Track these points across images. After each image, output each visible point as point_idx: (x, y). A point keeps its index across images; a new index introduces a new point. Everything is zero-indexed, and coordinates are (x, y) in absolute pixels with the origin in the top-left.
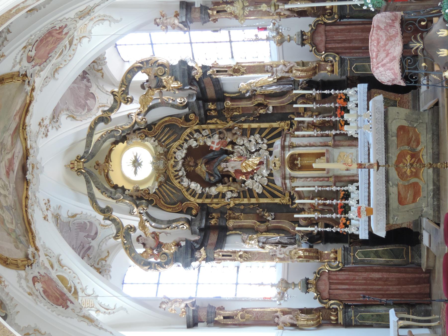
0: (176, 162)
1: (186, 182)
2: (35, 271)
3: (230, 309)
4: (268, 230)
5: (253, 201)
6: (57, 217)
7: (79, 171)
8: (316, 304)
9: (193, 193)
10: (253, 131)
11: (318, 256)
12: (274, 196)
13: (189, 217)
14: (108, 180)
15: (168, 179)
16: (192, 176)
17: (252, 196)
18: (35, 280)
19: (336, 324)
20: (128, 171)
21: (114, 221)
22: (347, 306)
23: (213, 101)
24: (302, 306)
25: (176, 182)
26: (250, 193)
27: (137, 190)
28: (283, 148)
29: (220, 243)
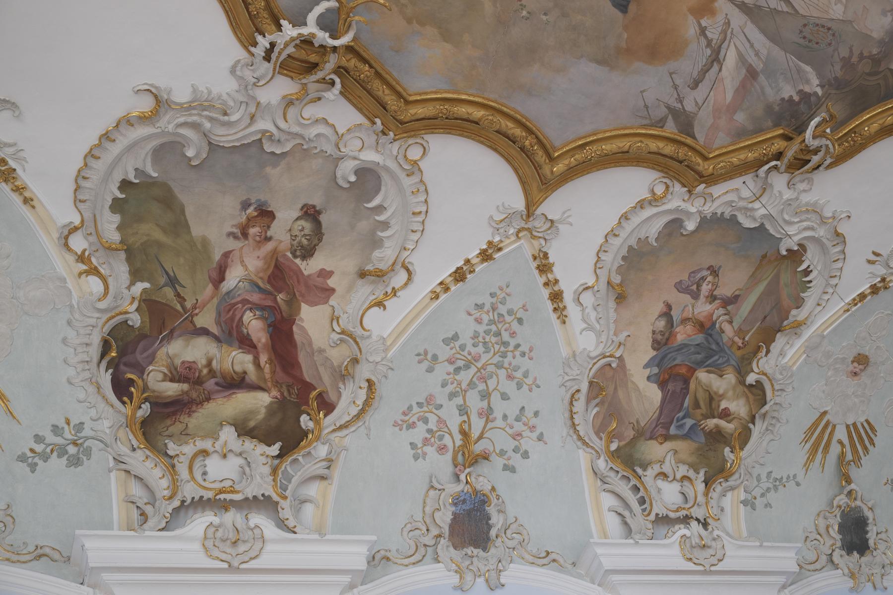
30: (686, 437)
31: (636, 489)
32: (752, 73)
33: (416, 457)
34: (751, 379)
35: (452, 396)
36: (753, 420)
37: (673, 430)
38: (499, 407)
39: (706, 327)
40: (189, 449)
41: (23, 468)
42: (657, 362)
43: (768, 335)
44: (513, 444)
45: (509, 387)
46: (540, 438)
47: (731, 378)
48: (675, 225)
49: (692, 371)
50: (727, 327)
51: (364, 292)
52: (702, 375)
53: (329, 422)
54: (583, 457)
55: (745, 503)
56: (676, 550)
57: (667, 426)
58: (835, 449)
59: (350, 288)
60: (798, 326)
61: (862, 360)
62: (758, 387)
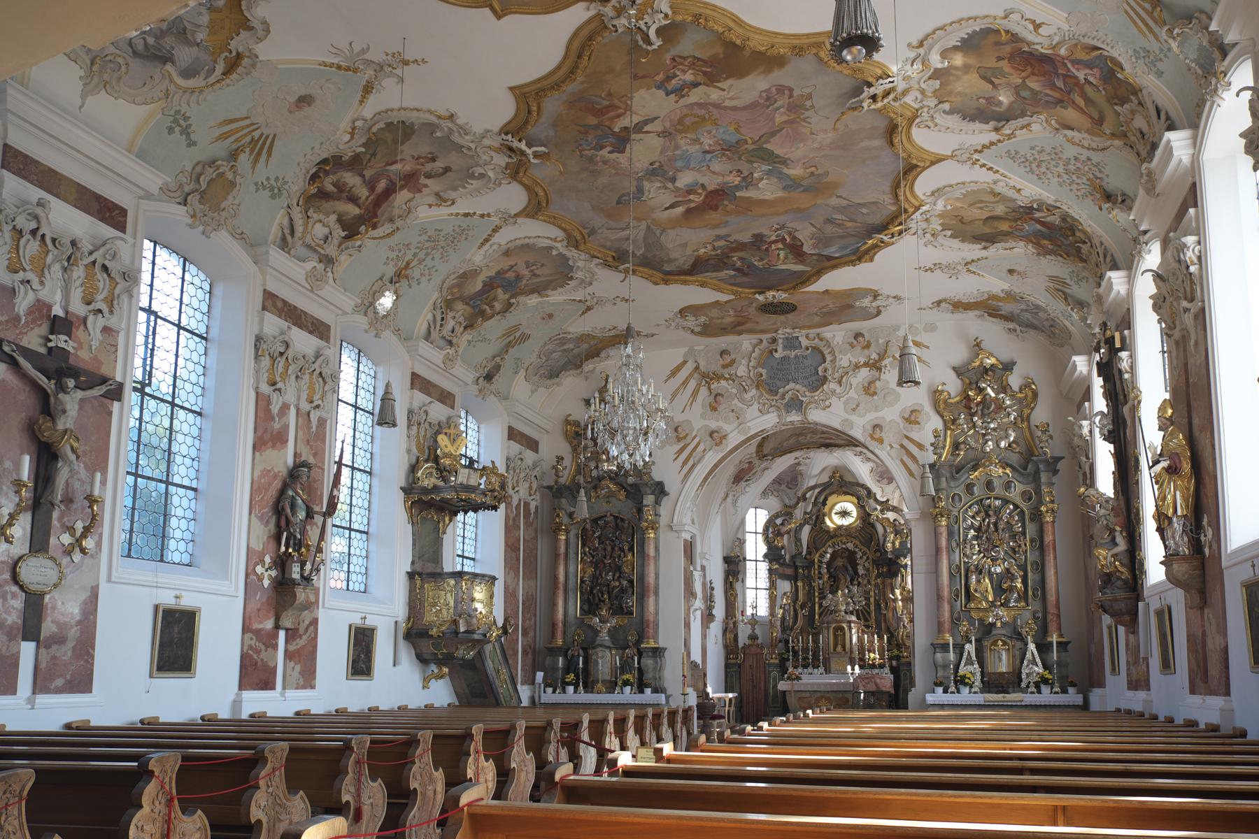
0: (844, 544)
1: (830, 550)
2: (756, 461)
3: (738, 586)
4: (795, 610)
5: (817, 600)
6: (799, 464)
7: (832, 477)
8: (741, 645)
9: (822, 556)
10: (867, 599)
11: (773, 646)
12: (820, 615)
13: (804, 553)
14: (831, 494)
15: (832, 537)
16: (834, 555)
17: (820, 599)
18: (750, 463)
19: (727, 658)
20: (838, 508)
21: (798, 503)
22: (739, 666)
23: (889, 570)
24: (740, 635)
25: (830, 543)
26: (822, 597)
27: (824, 515)
28: (850, 622)
29: (784, 577)
30: (473, 307)
31: (443, 319)
32: (628, 239)
33: (385, 263)
34: (513, 301)
35: (417, 248)
36: (499, 313)
37: (471, 303)
38: (429, 262)
39: (518, 278)
40: (316, 216)
41: (253, 187)
42: (491, 278)
43: (532, 292)
44: (419, 277)
45: (438, 256)
46: (429, 280)
47: (507, 296)
48: (551, 248)
49: (498, 287)
50: (524, 282)
51: (432, 200)
52: (500, 291)
53: (372, 233)
54: (436, 295)
55: (469, 341)
56: (442, 357)
57: (471, 300)
58: (512, 338)
59: (428, 195)
60: (547, 296)
61: (550, 316)
62: (511, 305)
